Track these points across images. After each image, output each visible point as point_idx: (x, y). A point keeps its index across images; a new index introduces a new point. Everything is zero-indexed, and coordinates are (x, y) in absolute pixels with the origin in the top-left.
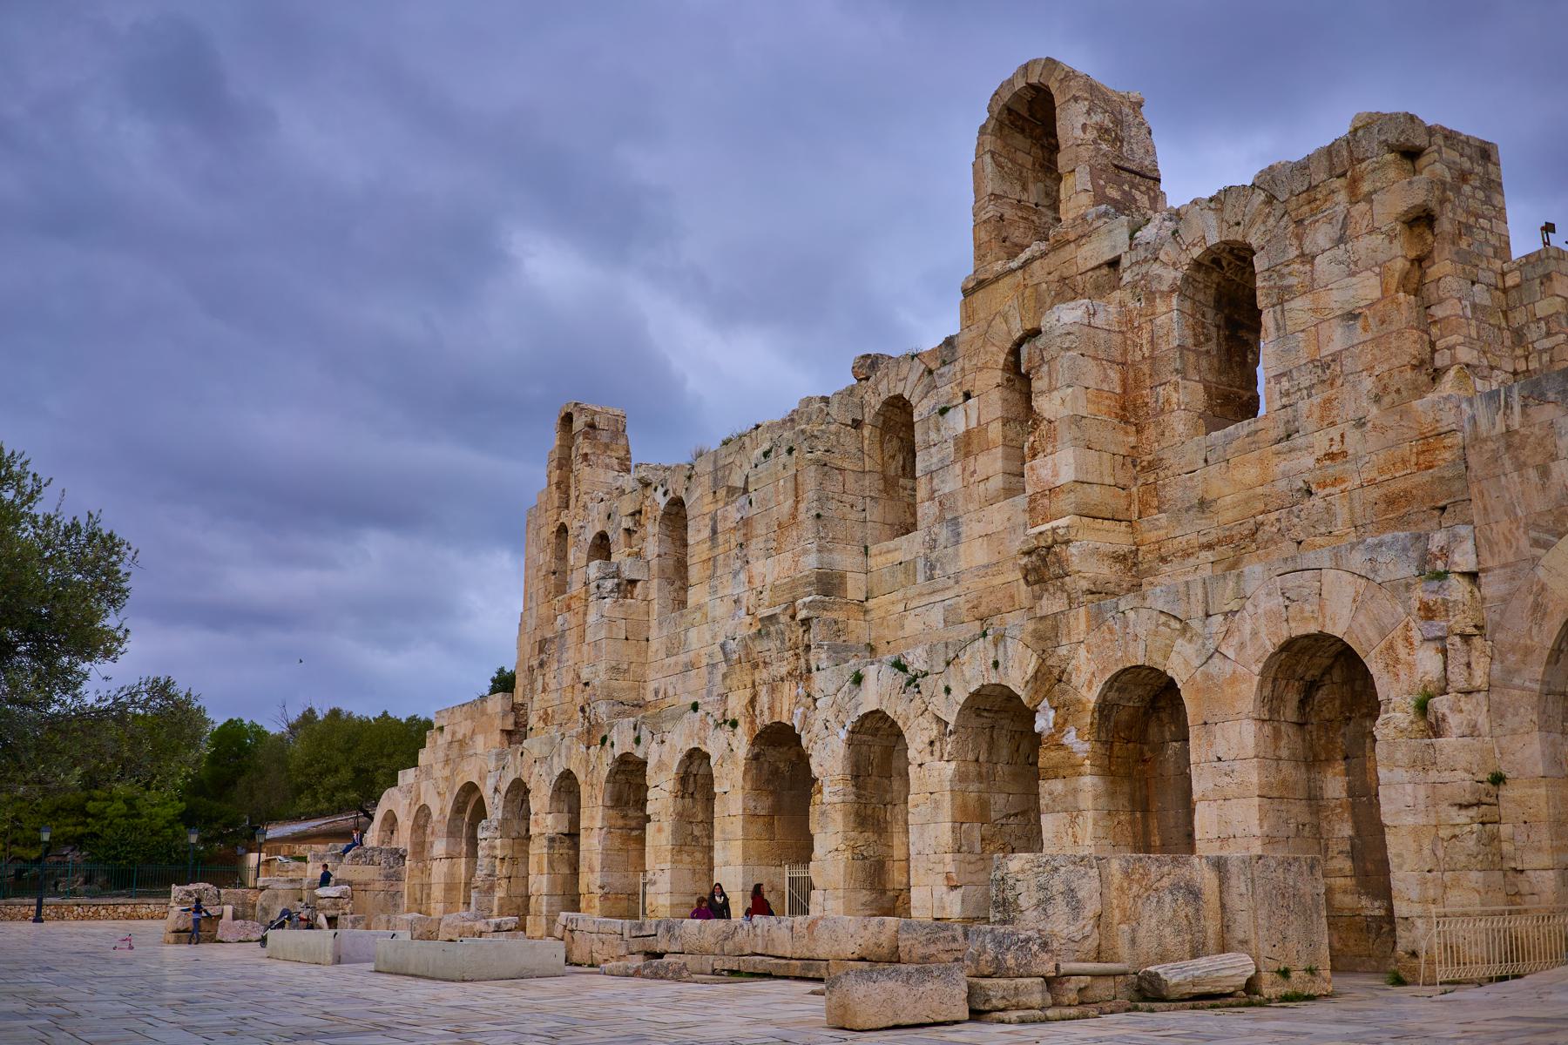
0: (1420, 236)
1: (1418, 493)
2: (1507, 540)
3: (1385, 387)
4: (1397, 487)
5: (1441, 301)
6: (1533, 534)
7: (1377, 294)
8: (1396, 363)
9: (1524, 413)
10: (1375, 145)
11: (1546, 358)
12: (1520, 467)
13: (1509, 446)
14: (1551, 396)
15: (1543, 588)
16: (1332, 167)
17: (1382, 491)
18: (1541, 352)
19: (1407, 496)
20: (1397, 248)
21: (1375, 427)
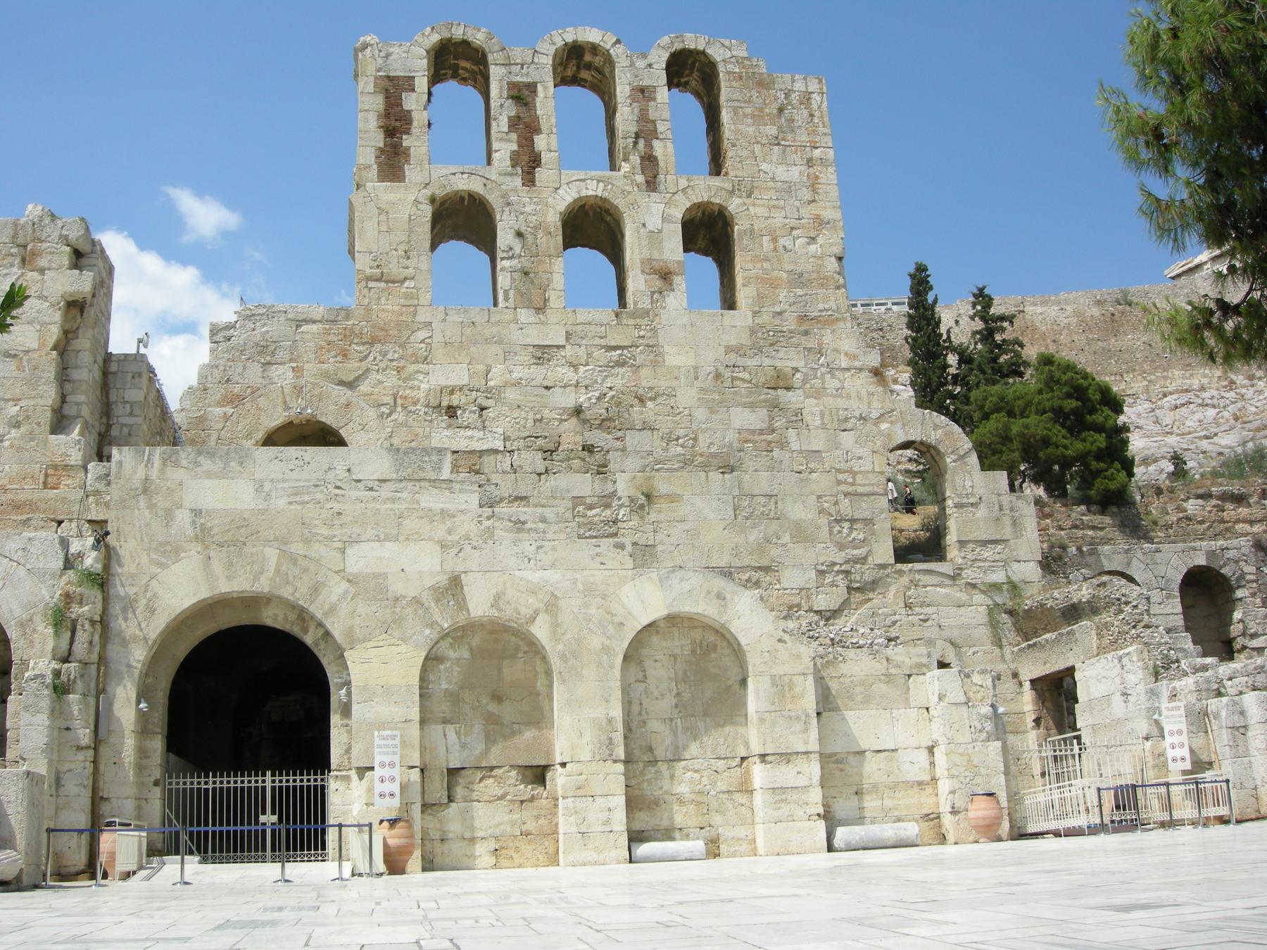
0: (74, 318)
1: (42, 506)
2: (132, 556)
3: (28, 418)
4: (23, 496)
5: (77, 367)
6: (154, 556)
7: (35, 345)
8: (42, 402)
9: (162, 471)
10: (56, 234)
11: (126, 430)
12: (151, 507)
13: (145, 491)
14: (184, 463)
15: (155, 595)
16: (15, 236)
17: (10, 496)
18: (123, 425)
19: (31, 506)
20: (58, 317)
21: (12, 446)
